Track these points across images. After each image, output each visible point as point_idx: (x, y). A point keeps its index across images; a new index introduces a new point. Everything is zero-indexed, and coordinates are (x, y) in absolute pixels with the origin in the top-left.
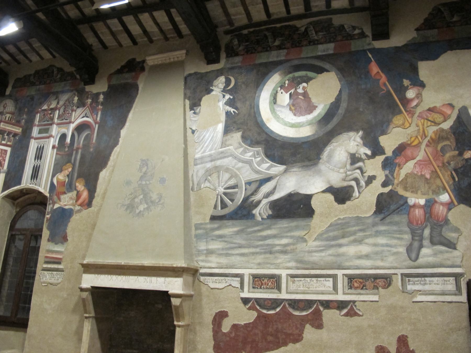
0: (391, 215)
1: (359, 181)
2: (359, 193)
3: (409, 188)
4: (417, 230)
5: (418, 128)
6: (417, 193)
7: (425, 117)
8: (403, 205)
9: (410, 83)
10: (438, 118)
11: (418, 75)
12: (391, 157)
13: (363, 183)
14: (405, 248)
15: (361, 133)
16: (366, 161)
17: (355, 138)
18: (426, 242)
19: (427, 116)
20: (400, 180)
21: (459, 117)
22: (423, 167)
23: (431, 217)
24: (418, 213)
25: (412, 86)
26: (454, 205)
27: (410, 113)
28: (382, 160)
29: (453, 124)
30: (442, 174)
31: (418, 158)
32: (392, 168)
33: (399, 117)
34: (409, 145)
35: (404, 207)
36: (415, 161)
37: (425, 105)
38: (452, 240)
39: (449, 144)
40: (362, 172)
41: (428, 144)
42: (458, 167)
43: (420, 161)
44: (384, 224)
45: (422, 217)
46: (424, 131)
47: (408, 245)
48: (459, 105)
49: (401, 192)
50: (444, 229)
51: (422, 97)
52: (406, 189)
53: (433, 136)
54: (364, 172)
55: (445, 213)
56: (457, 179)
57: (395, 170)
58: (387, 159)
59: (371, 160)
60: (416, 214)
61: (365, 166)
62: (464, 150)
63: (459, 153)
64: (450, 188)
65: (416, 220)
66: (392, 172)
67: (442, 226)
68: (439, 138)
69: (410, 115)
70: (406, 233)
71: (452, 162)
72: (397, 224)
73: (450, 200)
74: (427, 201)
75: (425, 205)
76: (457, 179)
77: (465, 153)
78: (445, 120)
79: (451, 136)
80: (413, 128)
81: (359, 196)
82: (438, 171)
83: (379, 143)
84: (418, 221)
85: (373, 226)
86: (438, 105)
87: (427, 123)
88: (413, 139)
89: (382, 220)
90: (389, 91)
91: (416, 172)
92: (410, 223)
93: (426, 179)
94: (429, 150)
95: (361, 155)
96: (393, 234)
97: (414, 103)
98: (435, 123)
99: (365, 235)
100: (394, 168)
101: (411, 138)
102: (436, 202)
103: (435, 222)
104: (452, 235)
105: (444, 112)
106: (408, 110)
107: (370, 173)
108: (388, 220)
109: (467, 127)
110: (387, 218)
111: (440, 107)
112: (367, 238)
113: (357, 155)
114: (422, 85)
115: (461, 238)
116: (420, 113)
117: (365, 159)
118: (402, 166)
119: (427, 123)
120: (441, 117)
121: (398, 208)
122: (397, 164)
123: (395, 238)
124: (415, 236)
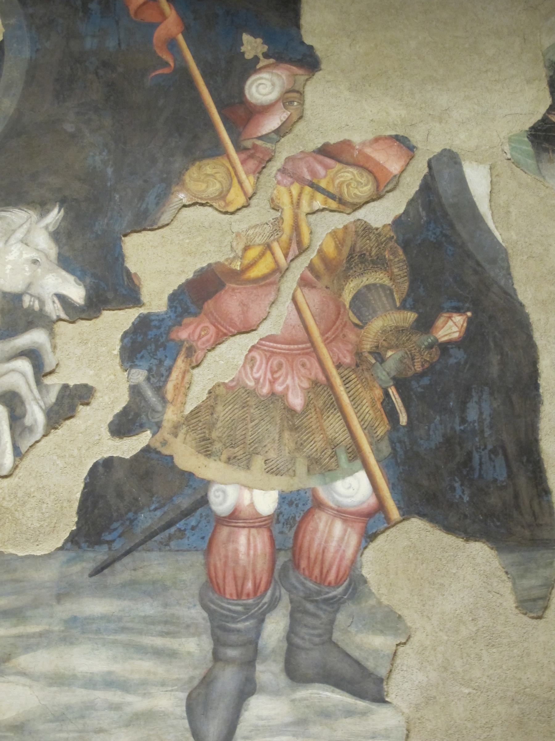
0: (136, 554)
1: (22, 403)
2: (18, 453)
3: (218, 446)
4: (234, 620)
5: (279, 214)
6: (248, 467)
7: (309, 177)
8: (187, 513)
9: (265, 48)
10: (352, 181)
11: (298, 26)
12: (161, 319)
13: (36, 415)
14: (184, 695)
15: (55, 215)
16: (62, 328)
17: (29, 231)
18: (269, 672)
19: (313, 173)
20: (189, 409)
21: (428, 187)
22: (280, 366)
23: (297, 566)
24: (247, 548)
25: (272, 61)
26: (387, 519)
27: (251, 157)
28: (127, 326)
29: (406, 212)
30: (353, 399)
31: (265, 330)
32: (161, 362)
33: (209, 167)
34: (236, 276)
35: (192, 521)
36: (252, 339)
37: (313, 133)
38: (370, 664)
39: (387, 282)
40: (40, 372)
41: (309, 274)
42: (410, 373)
43: (270, 338)
44: (103, 591)
45: (262, 565)
46: (296, 227)
47: (196, 682)
48: (430, 144)
49: (187, 458)
50: (341, 618)
51: (302, 103)
52: (206, 448)
53: (331, 250)
54: (48, 369)
55: (350, 553)
56: (403, 419)
57: (170, 370)
58: (143, 324)
59: (83, 325)
60: (236, 551)
61: (54, 347)
62: (439, 310)
63: (417, 321)
64: (376, 451)
65: (235, 578)
66: (158, 378)
67: (335, 604)
68: (350, 257)
69: (252, 164)
70: (190, 629)
71: (390, 353)
72: (155, 589)
73: (373, 501)
74: (285, 499)
75: (278, 515)
76: (403, 419)
77: (440, 322)
78: (377, 196)
79: (394, 253)
80: (258, 215)
81: (15, 467)
82: (337, 381)
83: (120, 258)
84: (245, 578)
85: (60, 597)
86: (357, 139)
87: (312, 198)
88: (252, 254)
89: (98, 571)
90: (183, 72)
91: (251, 384)
92: (212, 584)
93: (291, 411)
94: (310, 301)
95: (42, 303)
96: (140, 632)
97: (271, 123)
98: (341, 201)
99: (20, 636)
100: (167, 363)
101: (246, 248)
102: (318, 504)
103: (310, 584)
104: (369, 644)
105: (378, 164)
106: (248, 144)
107: (71, 375)
108: (123, 572)
109: (452, 226)
110: (118, 566)
111: (364, 144)
112: (28, 649)
113: (27, 301)
114: (309, 62)
115: (408, 657)
116: (288, 159)
117: (60, 319)
118: (200, 354)
119: (312, 198)
120: (363, 180)
121: (169, 525)
122: (180, 344)
123: (143, 651)
124: (225, 645)
